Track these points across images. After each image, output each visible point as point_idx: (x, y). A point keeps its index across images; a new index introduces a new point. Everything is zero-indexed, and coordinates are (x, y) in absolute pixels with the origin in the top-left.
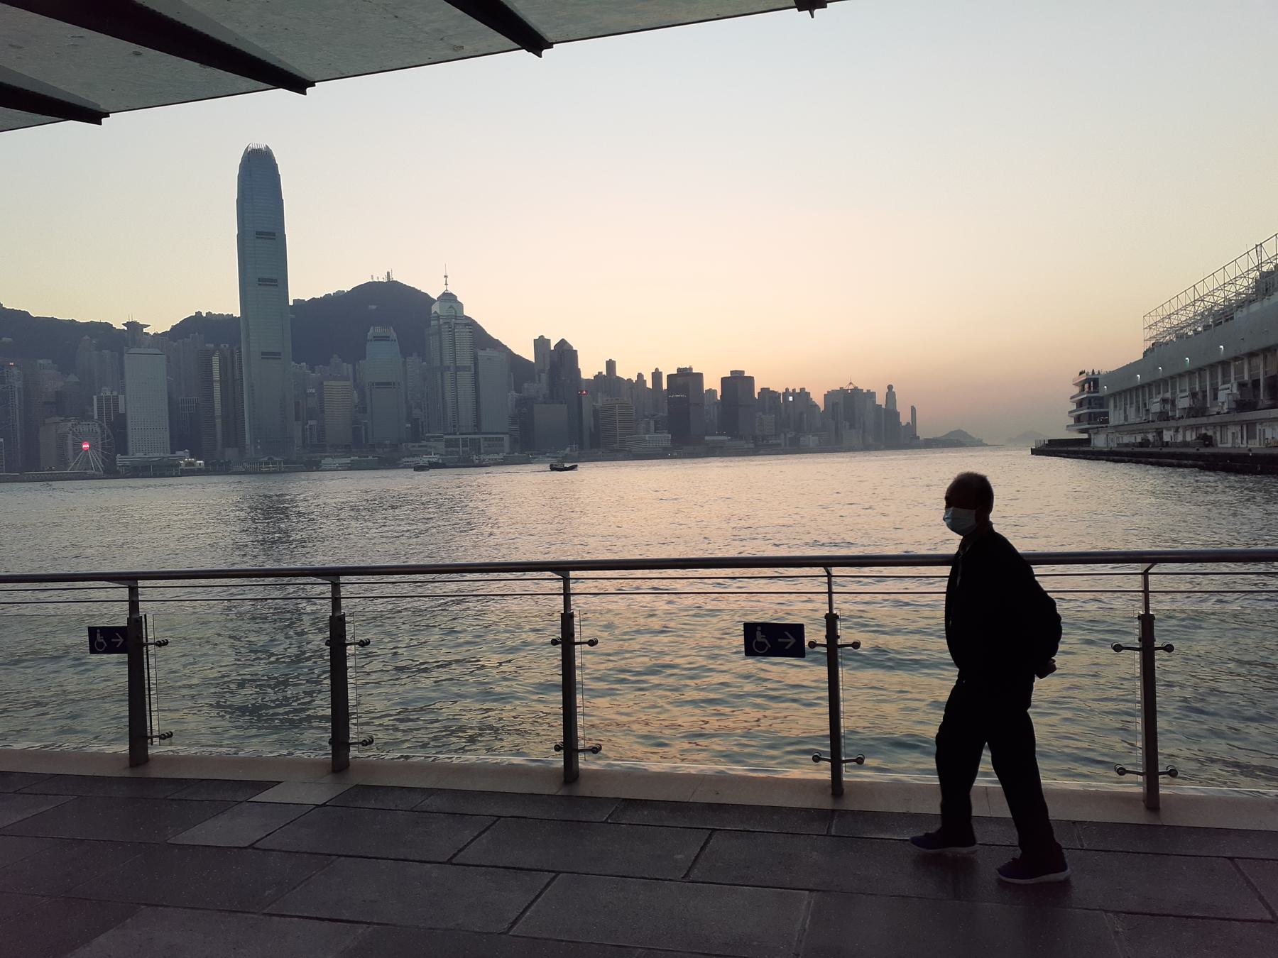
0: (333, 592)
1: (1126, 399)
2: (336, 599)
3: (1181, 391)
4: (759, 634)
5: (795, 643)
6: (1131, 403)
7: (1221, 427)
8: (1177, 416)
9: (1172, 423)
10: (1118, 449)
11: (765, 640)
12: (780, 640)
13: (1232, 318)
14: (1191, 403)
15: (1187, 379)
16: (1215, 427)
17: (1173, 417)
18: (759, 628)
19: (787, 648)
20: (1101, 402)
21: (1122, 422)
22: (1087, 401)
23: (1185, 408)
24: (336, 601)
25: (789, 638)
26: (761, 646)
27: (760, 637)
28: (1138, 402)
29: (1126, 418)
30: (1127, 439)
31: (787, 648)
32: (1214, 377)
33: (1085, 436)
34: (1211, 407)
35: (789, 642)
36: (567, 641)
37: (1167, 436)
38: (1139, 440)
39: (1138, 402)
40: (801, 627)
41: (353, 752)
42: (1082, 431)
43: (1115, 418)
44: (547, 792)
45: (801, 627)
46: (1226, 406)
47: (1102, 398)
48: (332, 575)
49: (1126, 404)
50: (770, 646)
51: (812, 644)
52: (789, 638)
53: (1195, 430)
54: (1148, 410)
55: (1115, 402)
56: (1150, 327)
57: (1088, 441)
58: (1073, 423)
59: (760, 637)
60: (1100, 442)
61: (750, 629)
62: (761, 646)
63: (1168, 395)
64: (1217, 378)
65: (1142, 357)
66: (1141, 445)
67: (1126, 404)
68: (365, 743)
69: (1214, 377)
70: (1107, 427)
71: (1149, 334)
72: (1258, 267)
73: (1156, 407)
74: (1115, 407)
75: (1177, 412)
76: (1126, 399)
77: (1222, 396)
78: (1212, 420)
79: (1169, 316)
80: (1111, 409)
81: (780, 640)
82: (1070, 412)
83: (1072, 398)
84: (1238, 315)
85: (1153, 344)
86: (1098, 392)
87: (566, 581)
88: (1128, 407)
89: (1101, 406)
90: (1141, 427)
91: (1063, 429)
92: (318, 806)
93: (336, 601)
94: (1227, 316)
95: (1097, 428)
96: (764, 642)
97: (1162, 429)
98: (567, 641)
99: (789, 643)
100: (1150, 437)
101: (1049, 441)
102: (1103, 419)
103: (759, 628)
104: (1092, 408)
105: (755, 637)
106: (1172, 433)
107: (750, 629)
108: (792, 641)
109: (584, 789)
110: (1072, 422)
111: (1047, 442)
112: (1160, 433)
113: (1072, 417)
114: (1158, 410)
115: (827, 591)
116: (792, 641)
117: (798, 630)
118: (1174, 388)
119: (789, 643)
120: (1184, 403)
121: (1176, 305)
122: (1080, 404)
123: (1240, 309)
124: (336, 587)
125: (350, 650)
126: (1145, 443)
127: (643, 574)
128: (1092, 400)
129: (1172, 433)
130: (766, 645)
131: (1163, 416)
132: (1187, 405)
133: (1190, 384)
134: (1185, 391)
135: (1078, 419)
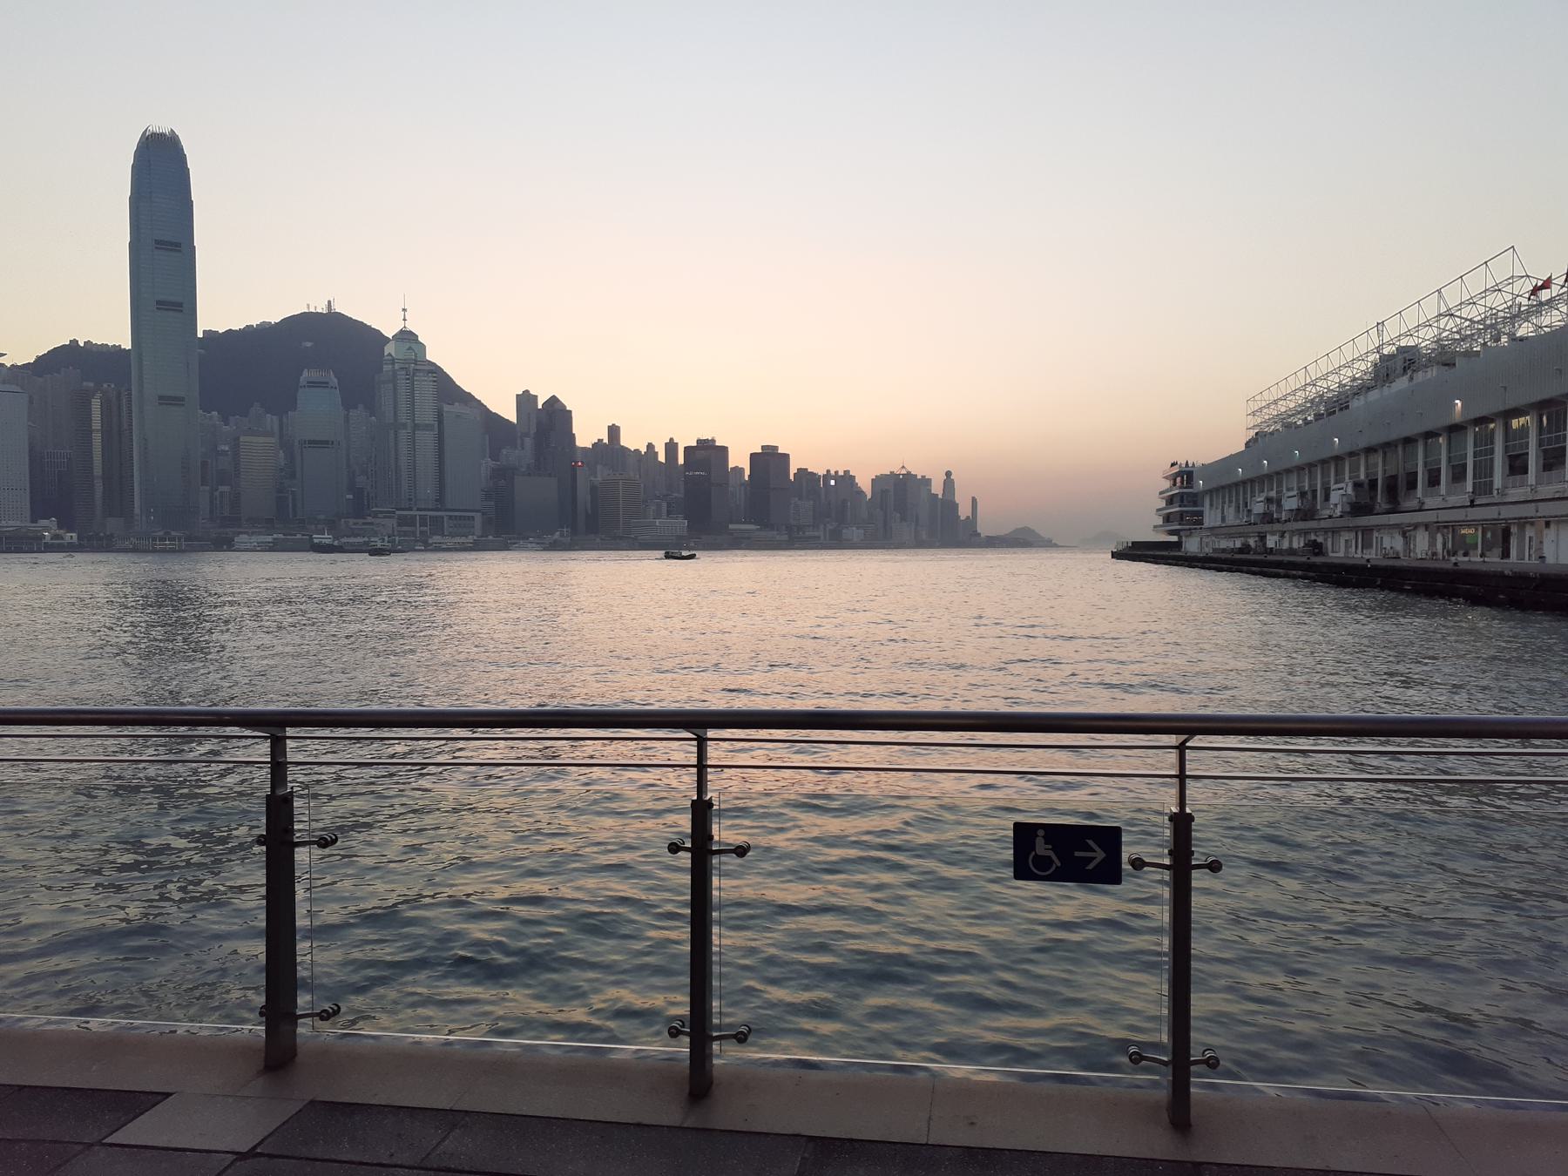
0: (273, 754)
1: (1224, 498)
2: (279, 763)
3: (1288, 490)
4: (1040, 842)
5: (1103, 860)
6: (1230, 502)
7: (1333, 532)
9: (1277, 527)
10: (1216, 555)
11: (1051, 854)
12: (1077, 854)
13: (1347, 407)
15: (1295, 474)
16: (1326, 532)
17: (1278, 521)
18: (1041, 832)
19: (1090, 867)
20: (1195, 499)
21: (1218, 523)
22: (1179, 498)
23: (1293, 510)
24: (278, 767)
25: (1095, 851)
26: (1043, 863)
27: (1041, 848)
28: (1237, 500)
29: (1223, 519)
30: (1225, 544)
31: (1090, 867)
32: (1325, 474)
33: (1174, 539)
34: (1322, 509)
35: (1094, 858)
36: (701, 848)
37: (1271, 542)
38: (1238, 545)
39: (1237, 500)
40: (1116, 832)
41: (303, 1029)
42: (1171, 533)
43: (1211, 518)
44: (666, 1122)
45: (1116, 832)
46: (1339, 509)
47: (1195, 495)
48: (274, 725)
49: (1224, 503)
50: (1059, 865)
51: (1138, 864)
52: (1095, 851)
53: (1303, 535)
54: (1249, 511)
55: (1211, 501)
56: (1254, 414)
57: (1178, 545)
58: (1161, 523)
59: (1041, 848)
60: (1192, 546)
61: (1024, 834)
62: (1043, 863)
63: (1273, 494)
64: (1329, 477)
65: (1243, 449)
66: (1241, 551)
67: (1224, 503)
68: (325, 1016)
69: (1325, 474)
70: (1201, 528)
71: (1252, 421)
72: (1378, 349)
73: (1259, 508)
74: (1211, 505)
75: (1284, 514)
76: (1224, 498)
77: (1335, 497)
78: (1323, 524)
79: (1275, 402)
81: (1077, 854)
82: (1158, 510)
83: (1161, 493)
84: (1355, 404)
85: (1257, 434)
86: (1192, 488)
87: (702, 743)
88: (1226, 506)
89: (1195, 504)
90: (1241, 530)
91: (1149, 529)
92: (241, 1156)
93: (278, 767)
94: (1341, 404)
95: (1190, 529)
96: (1049, 857)
98: (701, 848)
99: (1094, 858)
100: (1252, 542)
101: (1133, 543)
103: (1041, 832)
104: (1185, 506)
105: (1034, 849)
106: (1276, 538)
107: (1024, 834)
108: (1100, 855)
109: (727, 1114)
110: (1160, 521)
111: (1130, 545)
112: (1263, 538)
114: (1262, 511)
115: (1188, 781)
116: (1100, 855)
117: (1110, 838)
118: (1280, 485)
119: (1094, 858)
120: (1291, 503)
121: (1284, 389)
122: (1170, 501)
123: (1356, 397)
124: (278, 745)
125: (301, 855)
126: (1245, 549)
128: (1185, 497)
129: (1276, 538)
130: (1052, 862)
131: (1267, 518)
132: (1295, 506)
133: (1298, 482)
134: (1292, 489)
135: (1168, 519)
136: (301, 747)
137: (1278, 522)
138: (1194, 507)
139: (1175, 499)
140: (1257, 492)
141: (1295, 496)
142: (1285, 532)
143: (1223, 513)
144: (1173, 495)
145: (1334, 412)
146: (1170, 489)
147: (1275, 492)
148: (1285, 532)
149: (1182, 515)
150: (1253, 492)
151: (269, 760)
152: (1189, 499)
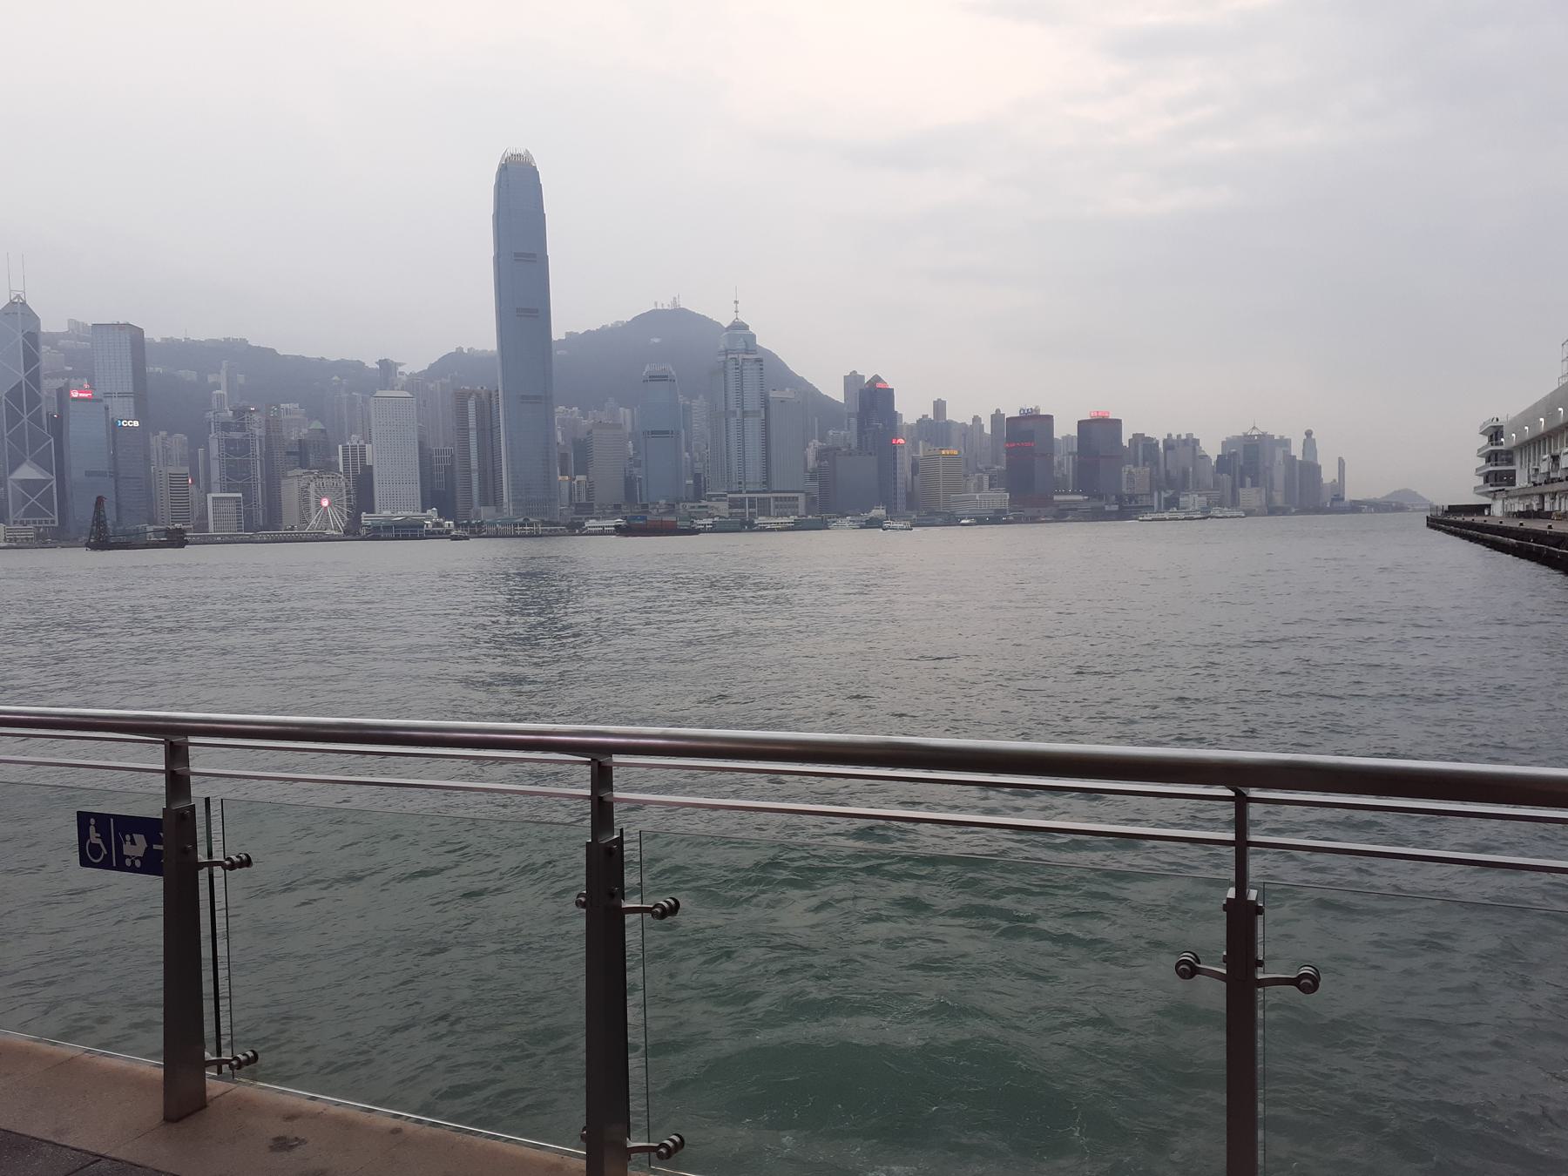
10: (1514, 524)
20: (1508, 456)
42: (1486, 494)
49: (1529, 461)
57: (1479, 509)
80: (1517, 467)
83: (1479, 450)
102: (1510, 478)
103: (92, 821)
104: (1501, 465)
110: (1481, 481)
111: (1446, 508)
113: (1480, 475)
136: (203, 758)
138: (1507, 465)
142: (1556, 493)
148: (1556, 493)
149: (1496, 475)
151: (164, 768)
152: (1503, 457)
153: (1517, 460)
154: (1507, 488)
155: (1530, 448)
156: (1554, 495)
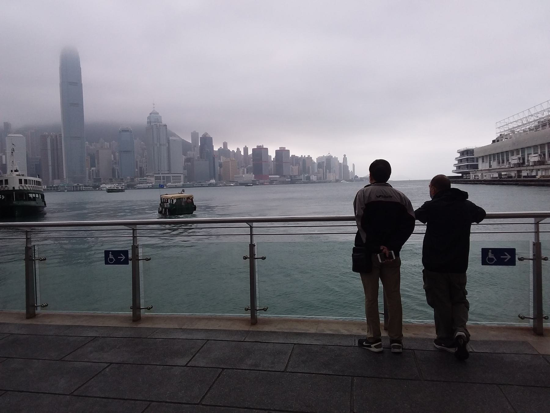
1: (490, 158)
6: (494, 160)
8: (531, 165)
9: (529, 168)
14: (539, 159)
20: (473, 160)
21: (488, 168)
22: (465, 160)
28: (498, 159)
29: (490, 166)
33: (460, 175)
43: (482, 166)
49: (490, 160)
53: (544, 170)
56: (499, 128)
58: (456, 169)
67: (490, 160)
74: (483, 162)
76: (490, 158)
82: (455, 164)
83: (456, 158)
85: (501, 135)
89: (473, 162)
90: (508, 170)
95: (475, 171)
97: (522, 170)
100: (513, 174)
106: (528, 172)
110: (455, 168)
112: (520, 172)
122: (460, 161)
127: (340, 229)
128: (469, 159)
131: (519, 165)
134: (531, 154)
135: (459, 167)
137: (529, 166)
139: (463, 160)
140: (510, 155)
141: (537, 156)
142: (533, 170)
143: (490, 163)
144: (462, 159)
145: (546, 125)
146: (460, 157)
147: (520, 154)
148: (533, 170)
150: (507, 156)
153: (480, 161)
154: (476, 170)
155: (498, 157)
156: (539, 170)
